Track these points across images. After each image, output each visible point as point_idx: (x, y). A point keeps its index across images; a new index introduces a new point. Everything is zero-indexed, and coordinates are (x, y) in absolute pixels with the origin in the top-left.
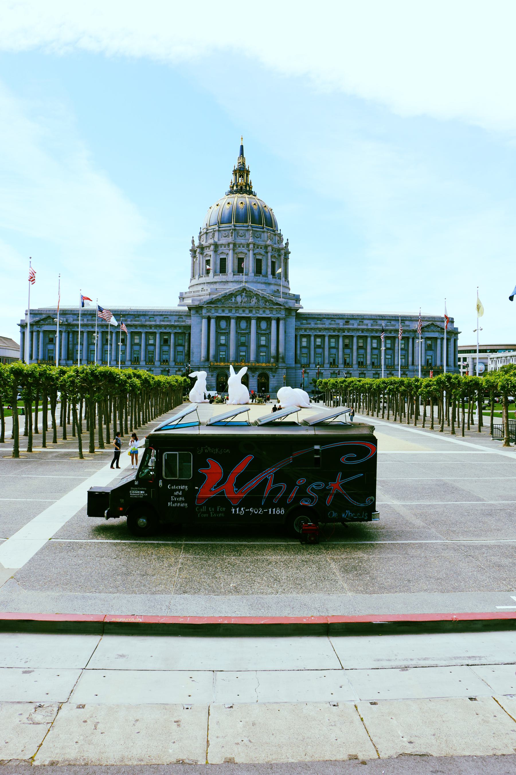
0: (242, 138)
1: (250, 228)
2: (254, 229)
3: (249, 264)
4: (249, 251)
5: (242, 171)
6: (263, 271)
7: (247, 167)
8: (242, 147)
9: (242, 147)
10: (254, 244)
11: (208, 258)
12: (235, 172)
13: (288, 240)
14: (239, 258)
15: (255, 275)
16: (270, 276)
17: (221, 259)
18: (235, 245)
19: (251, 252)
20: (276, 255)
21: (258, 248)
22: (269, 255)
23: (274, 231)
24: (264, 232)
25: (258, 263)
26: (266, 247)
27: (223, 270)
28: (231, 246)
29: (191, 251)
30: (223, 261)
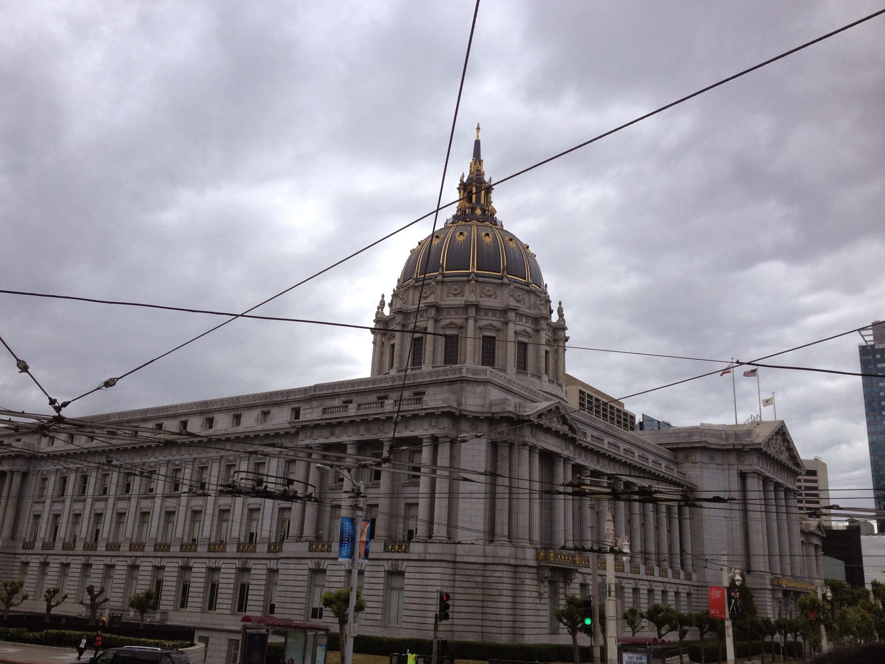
0: (478, 129)
2: (480, 279)
4: (467, 320)
6: (498, 360)
7: (486, 179)
8: (477, 144)
9: (477, 144)
12: (464, 187)
13: (560, 303)
19: (471, 322)
20: (530, 330)
21: (486, 315)
22: (511, 326)
24: (502, 284)
26: (505, 311)
28: (433, 312)
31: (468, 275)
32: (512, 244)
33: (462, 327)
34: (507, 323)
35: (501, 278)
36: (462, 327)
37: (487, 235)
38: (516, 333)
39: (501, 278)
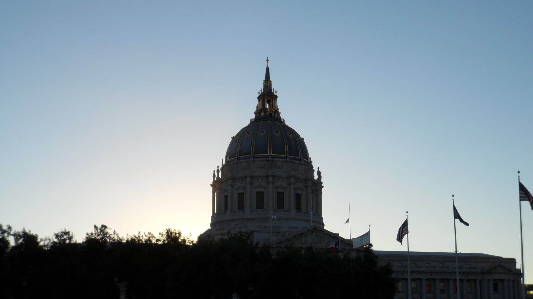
0: (268, 61)
1: (270, 158)
2: (274, 159)
3: (270, 200)
4: (269, 183)
5: (268, 96)
6: (286, 206)
8: (268, 70)
9: (268, 70)
10: (274, 177)
11: (226, 194)
12: (261, 98)
13: (318, 168)
14: (257, 192)
15: (274, 211)
16: (293, 211)
17: (239, 194)
18: (252, 177)
19: (271, 185)
22: (292, 186)
23: (300, 160)
25: (280, 196)
27: (241, 206)
28: (248, 179)
29: (211, 185)
30: (241, 196)
31: (268, 157)
32: (291, 136)
33: (265, 187)
34: (289, 184)
35: (286, 158)
36: (265, 187)
37: (277, 132)
38: (295, 189)
39: (286, 158)
